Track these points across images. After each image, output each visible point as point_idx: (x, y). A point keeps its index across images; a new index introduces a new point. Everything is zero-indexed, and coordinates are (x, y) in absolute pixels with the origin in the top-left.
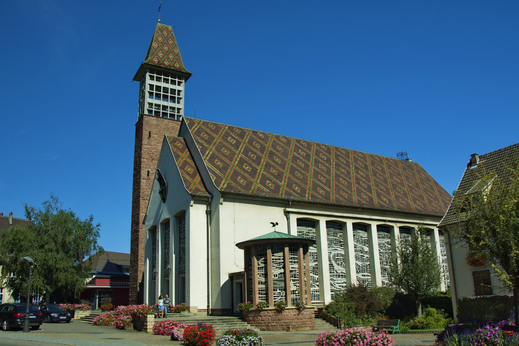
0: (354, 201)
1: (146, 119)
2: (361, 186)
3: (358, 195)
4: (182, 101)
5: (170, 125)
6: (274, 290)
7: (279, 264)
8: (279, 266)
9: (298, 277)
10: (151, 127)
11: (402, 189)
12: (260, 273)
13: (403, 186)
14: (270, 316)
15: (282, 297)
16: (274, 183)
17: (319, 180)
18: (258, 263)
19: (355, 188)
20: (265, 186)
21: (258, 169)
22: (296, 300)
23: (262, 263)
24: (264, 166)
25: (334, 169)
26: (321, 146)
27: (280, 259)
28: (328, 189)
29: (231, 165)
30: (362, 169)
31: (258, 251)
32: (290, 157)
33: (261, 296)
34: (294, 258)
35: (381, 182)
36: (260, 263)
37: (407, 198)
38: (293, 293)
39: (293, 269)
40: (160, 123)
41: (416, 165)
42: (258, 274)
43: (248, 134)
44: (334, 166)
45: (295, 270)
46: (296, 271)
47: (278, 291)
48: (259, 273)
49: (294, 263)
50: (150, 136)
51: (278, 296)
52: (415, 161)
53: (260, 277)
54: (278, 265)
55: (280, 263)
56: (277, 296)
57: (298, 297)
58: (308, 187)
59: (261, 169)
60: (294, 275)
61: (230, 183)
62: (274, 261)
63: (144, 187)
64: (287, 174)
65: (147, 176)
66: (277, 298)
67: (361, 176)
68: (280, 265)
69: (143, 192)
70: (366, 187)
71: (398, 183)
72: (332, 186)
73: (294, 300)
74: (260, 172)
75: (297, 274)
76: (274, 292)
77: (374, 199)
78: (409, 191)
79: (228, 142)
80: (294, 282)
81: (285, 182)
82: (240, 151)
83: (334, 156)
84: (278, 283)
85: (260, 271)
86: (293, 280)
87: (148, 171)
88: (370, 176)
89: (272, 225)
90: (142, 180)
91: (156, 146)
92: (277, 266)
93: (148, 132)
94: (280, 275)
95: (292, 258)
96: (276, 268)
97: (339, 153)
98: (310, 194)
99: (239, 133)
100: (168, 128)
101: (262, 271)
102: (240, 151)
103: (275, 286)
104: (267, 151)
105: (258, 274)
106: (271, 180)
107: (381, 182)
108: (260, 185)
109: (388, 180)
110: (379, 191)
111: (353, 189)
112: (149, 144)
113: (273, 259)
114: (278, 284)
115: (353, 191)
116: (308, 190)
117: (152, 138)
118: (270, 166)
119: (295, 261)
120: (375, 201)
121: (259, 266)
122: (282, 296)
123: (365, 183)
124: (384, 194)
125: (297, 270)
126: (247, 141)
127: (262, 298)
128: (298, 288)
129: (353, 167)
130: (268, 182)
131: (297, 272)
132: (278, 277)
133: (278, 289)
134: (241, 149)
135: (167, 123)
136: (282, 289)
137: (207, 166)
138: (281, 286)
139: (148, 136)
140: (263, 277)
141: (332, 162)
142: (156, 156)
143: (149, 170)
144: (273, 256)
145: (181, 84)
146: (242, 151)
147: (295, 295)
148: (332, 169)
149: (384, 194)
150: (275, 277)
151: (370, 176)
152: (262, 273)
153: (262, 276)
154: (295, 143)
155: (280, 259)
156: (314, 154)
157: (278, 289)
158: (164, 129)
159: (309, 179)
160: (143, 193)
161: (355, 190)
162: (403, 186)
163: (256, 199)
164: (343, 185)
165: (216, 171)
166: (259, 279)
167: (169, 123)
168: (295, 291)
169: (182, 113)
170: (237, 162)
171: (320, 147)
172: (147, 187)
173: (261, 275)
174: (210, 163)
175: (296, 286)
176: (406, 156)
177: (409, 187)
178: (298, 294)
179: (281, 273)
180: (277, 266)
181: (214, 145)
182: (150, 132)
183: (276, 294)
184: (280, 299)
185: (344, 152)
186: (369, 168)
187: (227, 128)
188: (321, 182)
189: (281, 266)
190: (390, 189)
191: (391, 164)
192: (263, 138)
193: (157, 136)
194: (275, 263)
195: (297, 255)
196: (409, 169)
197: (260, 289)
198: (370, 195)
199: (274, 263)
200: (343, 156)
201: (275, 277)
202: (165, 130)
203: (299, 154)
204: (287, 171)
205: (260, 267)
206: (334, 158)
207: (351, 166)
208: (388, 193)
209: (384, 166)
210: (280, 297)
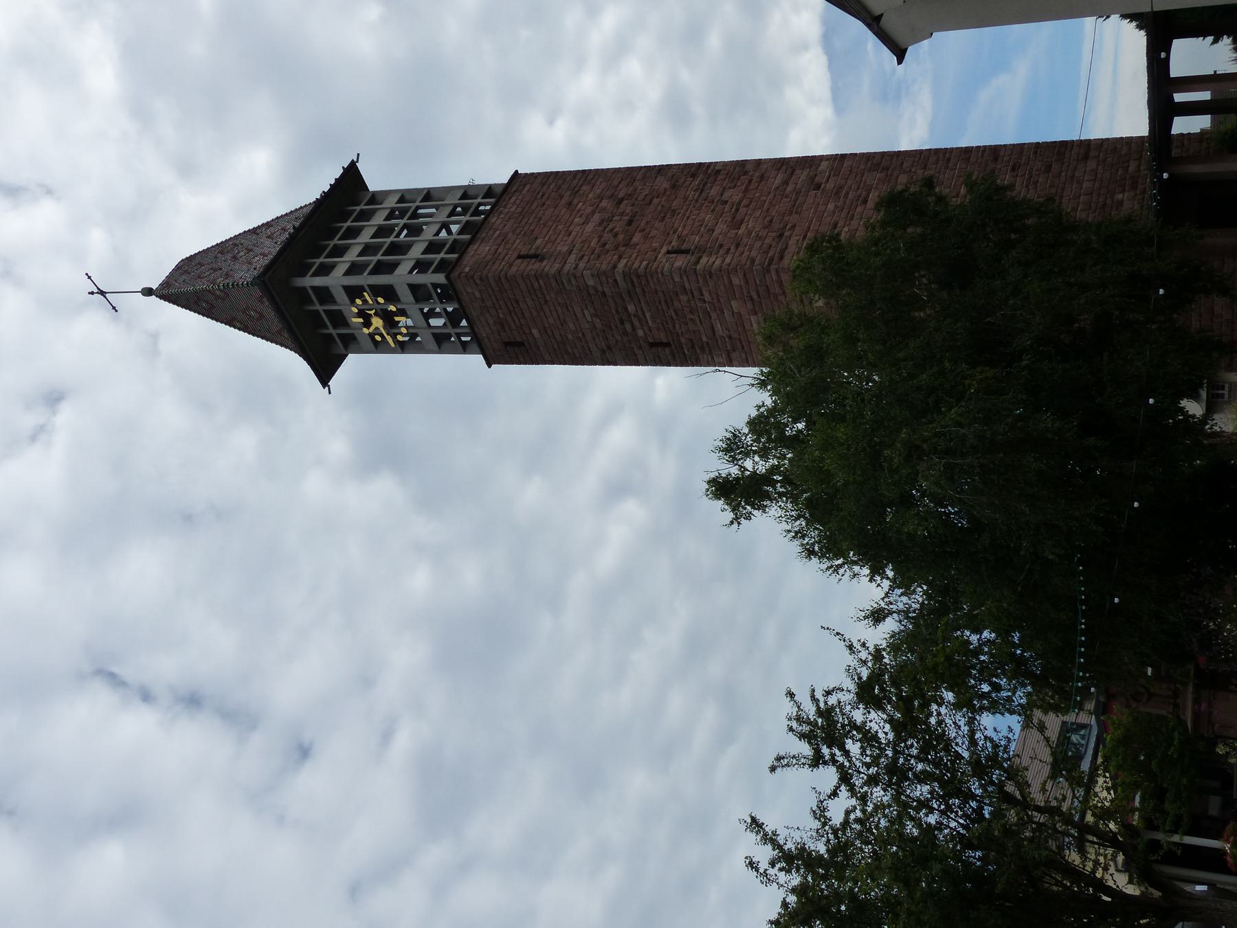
50: (535, 256)
69: (748, 263)
93: (520, 260)
117: (545, 250)
143: (664, 250)
182: (519, 257)
193: (539, 241)
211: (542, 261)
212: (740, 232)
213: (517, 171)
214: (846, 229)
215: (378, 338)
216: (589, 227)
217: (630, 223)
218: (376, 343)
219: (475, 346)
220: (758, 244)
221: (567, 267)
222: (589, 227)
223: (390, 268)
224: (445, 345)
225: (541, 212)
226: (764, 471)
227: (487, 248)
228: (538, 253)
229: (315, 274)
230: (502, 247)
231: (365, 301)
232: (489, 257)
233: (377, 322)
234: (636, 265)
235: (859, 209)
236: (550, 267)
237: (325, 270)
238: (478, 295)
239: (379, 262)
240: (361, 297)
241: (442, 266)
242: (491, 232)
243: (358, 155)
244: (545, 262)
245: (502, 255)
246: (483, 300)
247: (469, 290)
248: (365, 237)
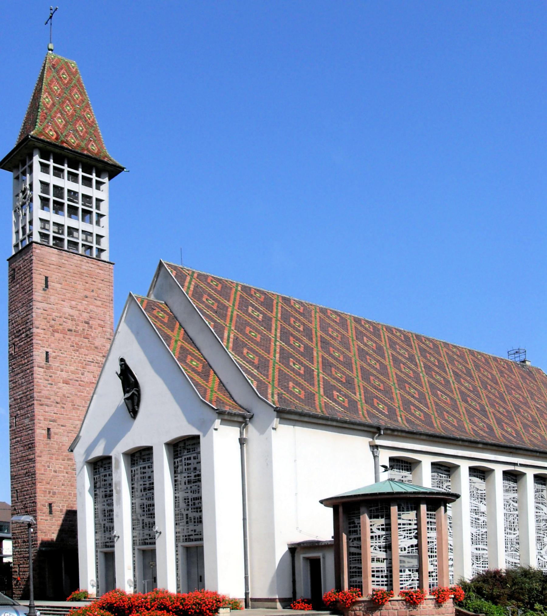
0: (468, 431)
1: (38, 251)
2: (470, 405)
3: (470, 421)
4: (104, 221)
5: (84, 267)
6: (401, 571)
7: (408, 532)
8: (409, 535)
9: (436, 552)
10: (48, 268)
11: (528, 413)
12: (374, 544)
13: (529, 407)
14: (397, 610)
15: (413, 582)
16: (346, 396)
17: (409, 394)
18: (371, 529)
19: (464, 409)
20: (335, 401)
21: (313, 370)
22: (433, 585)
23: (379, 529)
24: (320, 364)
25: (425, 374)
26: (394, 332)
27: (410, 524)
28: (426, 410)
29: (272, 361)
30: (464, 376)
31: (371, 510)
32: (354, 349)
33: (375, 579)
34: (431, 522)
35: (497, 400)
36: (374, 529)
37: (539, 428)
38: (430, 576)
39: (429, 540)
40: (66, 262)
41: (538, 371)
42: (372, 546)
43: (277, 303)
44: (423, 369)
45: (432, 540)
46: (433, 542)
47: (407, 572)
48: (372, 544)
49: (432, 530)
51: (407, 580)
52: (536, 365)
53: (375, 551)
54: (407, 533)
55: (410, 530)
56: (404, 581)
57: (435, 581)
58: (397, 405)
59: (318, 369)
60: (431, 549)
61: (282, 394)
62: (402, 526)
63: (40, 381)
64: (358, 381)
65: (45, 362)
66: (406, 582)
67: (465, 387)
68: (410, 533)
70: (478, 407)
71: (520, 401)
72: (429, 404)
73: (430, 585)
74: (318, 376)
75: (435, 547)
76: (401, 574)
77: (494, 428)
78: (539, 417)
79: (250, 315)
80: (431, 559)
81: (360, 395)
82: (276, 335)
83: (419, 352)
84: (406, 560)
85: (374, 541)
86: (429, 556)
87: (47, 353)
88: (479, 388)
89: (383, 469)
90: (36, 368)
91: (59, 306)
92: (407, 535)
94: (411, 549)
95: (428, 523)
96: (405, 538)
97: (422, 345)
98: (403, 417)
99: (262, 300)
100: (81, 273)
101: (379, 541)
102: (276, 335)
103: (402, 564)
104: (317, 336)
105: (372, 546)
106: (339, 391)
107: (497, 400)
108: (325, 399)
109: (505, 396)
110: (499, 415)
111: (461, 411)
112: (45, 300)
113: (399, 524)
114: (406, 562)
115: (462, 413)
116: (397, 410)
118: (331, 365)
119: (432, 527)
120: (496, 431)
121: (373, 534)
122: (413, 580)
123: (475, 400)
124: (506, 420)
125: (434, 540)
126: (279, 315)
127: (383, 583)
128: (435, 568)
129: (451, 371)
130: (336, 393)
131: (435, 543)
132: (407, 551)
133: (407, 570)
134: (276, 330)
135: (79, 262)
136: (413, 570)
137: (236, 361)
138: (411, 565)
140: (381, 551)
141: (418, 361)
142: (60, 325)
143: (48, 350)
144: (400, 518)
145: (102, 187)
146: (279, 335)
147: (431, 578)
148: (421, 375)
149: (506, 420)
150: (402, 551)
151: (479, 388)
152: (378, 544)
153: (379, 549)
154: (354, 324)
155: (410, 524)
156: (388, 346)
157: (407, 570)
158: (73, 274)
159: (393, 390)
160: (40, 392)
161: (465, 412)
162: (529, 407)
163: (329, 423)
164: (445, 403)
165: (252, 370)
166: (373, 555)
167: (83, 263)
168: (432, 572)
169: (105, 244)
170: (278, 355)
171: (392, 334)
172: (47, 382)
173: (377, 548)
174: (238, 356)
175: (433, 566)
176: (524, 356)
177: (537, 410)
178: (435, 578)
179: (412, 546)
180: (407, 535)
181: (231, 320)
183: (403, 576)
184: (410, 585)
185: (431, 345)
186: (473, 375)
187: (239, 288)
188: (413, 397)
189: (413, 534)
190: (513, 412)
191: (503, 369)
192: (301, 311)
193: (60, 286)
194: (403, 531)
195: (435, 518)
196: (530, 379)
197: (375, 569)
198: (487, 421)
199: (402, 530)
200: (431, 351)
201: (402, 551)
202: (75, 275)
203: (366, 345)
204: (357, 376)
205: (376, 536)
206: (419, 355)
207: (447, 369)
208: (512, 420)
209: (494, 373)
210: (410, 582)
217: (70, 330)
225: (81, 283)
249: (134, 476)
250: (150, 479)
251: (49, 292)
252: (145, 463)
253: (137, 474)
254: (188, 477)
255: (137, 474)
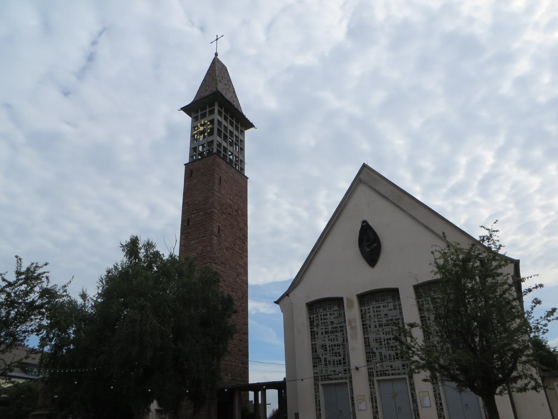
50: (220, 182)
69: (214, 253)
87: (219, 226)
93: (219, 177)
117: (222, 186)
139: (219, 182)
142: (226, 209)
143: (220, 225)
182: (220, 177)
193: (225, 184)
211: (219, 185)
212: (224, 250)
213: (248, 178)
214: (223, 285)
215: (196, 128)
216: (229, 201)
218: (195, 128)
219: (192, 160)
220: (220, 256)
221: (216, 193)
222: (229, 201)
223: (219, 135)
224: (192, 150)
226: (140, 256)
227: (224, 167)
228: (222, 184)
229: (219, 110)
230: (224, 172)
231: (209, 125)
232: (221, 167)
233: (201, 129)
234: (215, 215)
235: (230, 289)
236: (216, 187)
237: (220, 113)
238: (209, 163)
239: (221, 131)
240: (210, 124)
241: (219, 152)
242: (229, 169)
243: (256, 128)
244: (218, 186)
245: (221, 171)
246: (206, 164)
247: (210, 160)
248: (230, 128)
249: (365, 314)
250: (386, 317)
251: (221, 187)
252: (378, 303)
253: (369, 312)
254: (325, 329)
255: (369, 312)
